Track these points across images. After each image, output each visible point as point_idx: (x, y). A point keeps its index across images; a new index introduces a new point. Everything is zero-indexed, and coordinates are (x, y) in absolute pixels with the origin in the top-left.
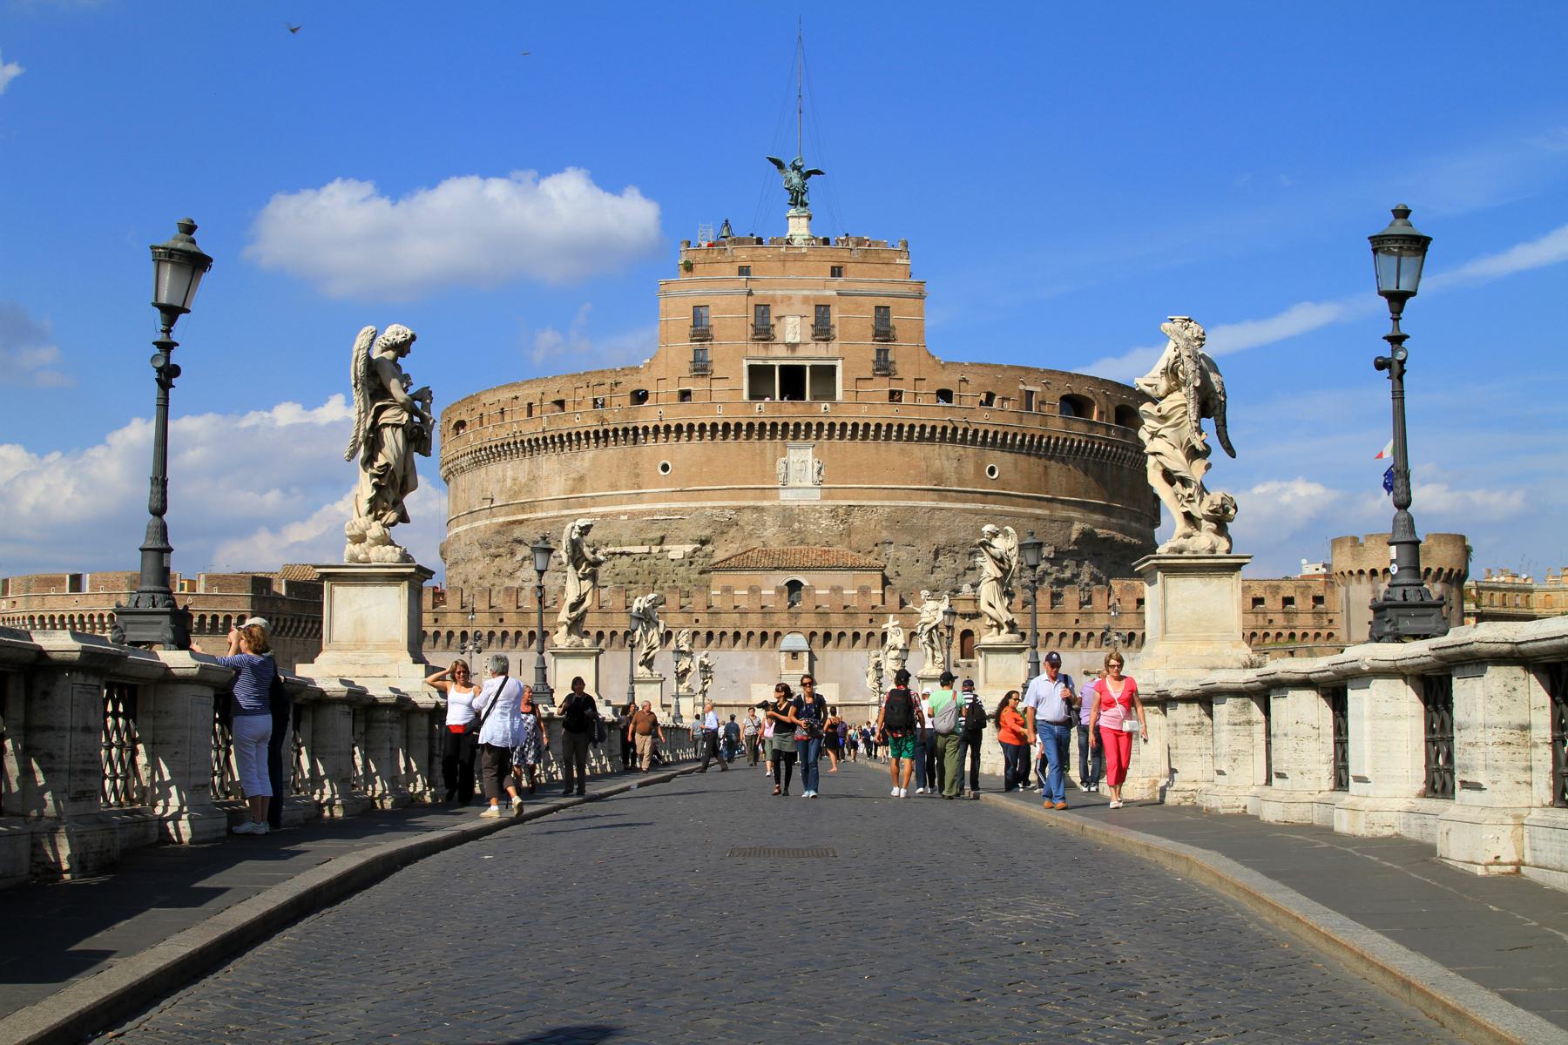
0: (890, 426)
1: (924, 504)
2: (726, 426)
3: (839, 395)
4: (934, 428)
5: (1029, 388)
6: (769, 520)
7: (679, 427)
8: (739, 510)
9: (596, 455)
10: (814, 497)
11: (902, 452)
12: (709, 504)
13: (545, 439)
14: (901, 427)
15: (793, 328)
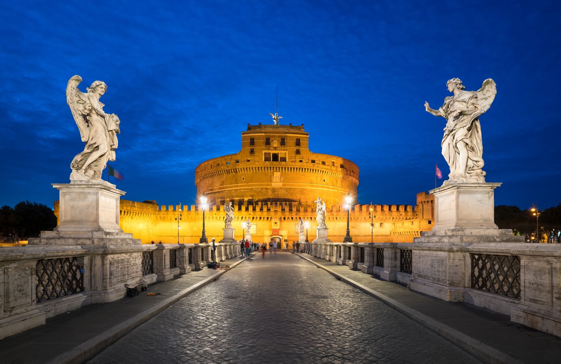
0: (300, 169)
1: (308, 188)
2: (258, 168)
3: (287, 160)
4: (310, 169)
5: (334, 161)
6: (269, 191)
7: (246, 169)
8: (262, 189)
9: (227, 176)
10: (280, 184)
11: (303, 175)
12: (255, 187)
13: (215, 173)
14: (302, 169)
15: (275, 143)
